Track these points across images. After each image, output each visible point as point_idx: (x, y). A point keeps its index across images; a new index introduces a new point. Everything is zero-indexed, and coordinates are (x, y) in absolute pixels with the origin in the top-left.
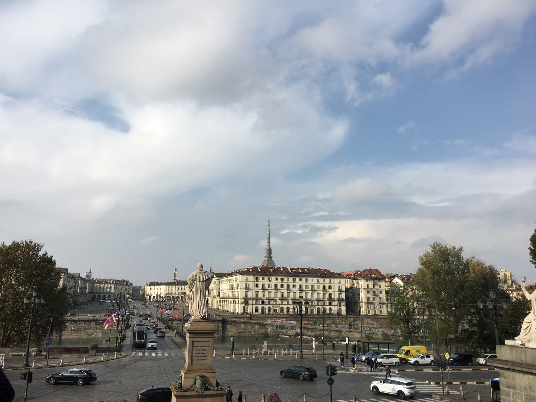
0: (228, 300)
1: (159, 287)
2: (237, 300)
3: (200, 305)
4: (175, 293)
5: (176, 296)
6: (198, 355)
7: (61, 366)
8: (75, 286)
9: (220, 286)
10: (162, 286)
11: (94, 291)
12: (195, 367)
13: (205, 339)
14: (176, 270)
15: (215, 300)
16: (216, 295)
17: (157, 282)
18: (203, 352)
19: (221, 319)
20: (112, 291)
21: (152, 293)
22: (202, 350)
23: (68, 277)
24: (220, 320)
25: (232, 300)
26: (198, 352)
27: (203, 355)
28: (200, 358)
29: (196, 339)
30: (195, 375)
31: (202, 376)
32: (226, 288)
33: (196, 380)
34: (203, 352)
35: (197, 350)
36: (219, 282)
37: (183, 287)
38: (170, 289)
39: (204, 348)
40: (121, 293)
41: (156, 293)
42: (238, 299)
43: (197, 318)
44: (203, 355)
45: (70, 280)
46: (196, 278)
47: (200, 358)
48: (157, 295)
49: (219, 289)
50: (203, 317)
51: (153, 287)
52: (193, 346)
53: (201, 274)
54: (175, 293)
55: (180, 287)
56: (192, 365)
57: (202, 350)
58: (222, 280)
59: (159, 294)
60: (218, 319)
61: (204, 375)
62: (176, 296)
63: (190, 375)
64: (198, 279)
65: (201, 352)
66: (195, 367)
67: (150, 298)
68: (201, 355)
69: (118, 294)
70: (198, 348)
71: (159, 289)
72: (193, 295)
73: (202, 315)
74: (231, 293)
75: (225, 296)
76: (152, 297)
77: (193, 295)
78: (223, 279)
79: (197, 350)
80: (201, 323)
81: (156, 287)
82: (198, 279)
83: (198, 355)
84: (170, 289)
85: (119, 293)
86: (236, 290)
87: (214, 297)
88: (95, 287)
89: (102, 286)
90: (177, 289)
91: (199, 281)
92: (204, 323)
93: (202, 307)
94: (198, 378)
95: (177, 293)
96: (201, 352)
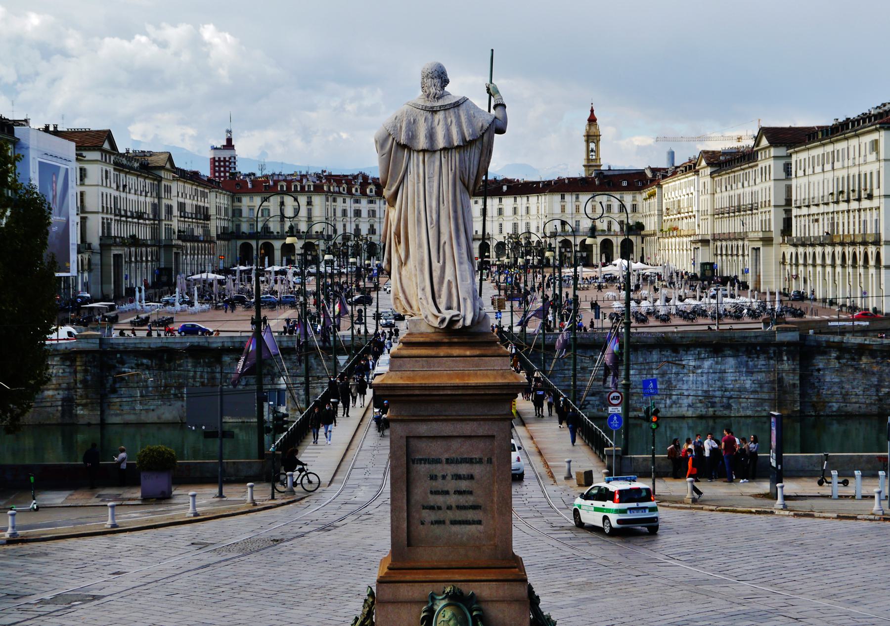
0: (829, 249)
1: (522, 201)
2: (872, 250)
3: (436, 266)
6: (440, 500)
7: (9, 542)
8: (156, 208)
9: (789, 189)
10: (533, 199)
11: (245, 228)
12: (425, 555)
13: (467, 428)
14: (592, 120)
15: (770, 255)
16: (776, 228)
17: (506, 181)
18: (464, 485)
19: (793, 336)
20: (317, 228)
21: (492, 228)
22: (458, 477)
23: (119, 167)
24: (789, 344)
25: (849, 250)
26: (439, 484)
27: (463, 500)
28: (450, 515)
29: (423, 429)
30: (428, 589)
31: (457, 599)
32: (817, 193)
33: (431, 611)
34: (464, 485)
35: (433, 477)
36: (787, 169)
37: (628, 199)
38: (569, 208)
39: (463, 469)
40: (358, 230)
41: (508, 229)
42: (877, 243)
43: (424, 328)
44: (463, 500)
45: (132, 180)
46: (412, 137)
47: (450, 515)
48: (515, 235)
49: (789, 202)
50: (452, 322)
52: (411, 460)
53: (440, 116)
56: (409, 545)
57: (458, 477)
58: (800, 157)
59: (522, 230)
60: (779, 337)
61: (469, 589)
63: (406, 592)
64: (422, 142)
65: (451, 485)
66: (425, 555)
68: (453, 499)
69: (346, 238)
70: (438, 469)
71: (522, 210)
72: (403, 220)
73: (448, 315)
74: (841, 219)
75: (818, 231)
76: (493, 244)
77: (403, 220)
78: (803, 156)
79: (433, 477)
80: (442, 351)
81: (508, 202)
82: (422, 142)
83: (440, 500)
84: (569, 208)
85: (350, 229)
86: (865, 204)
87: (767, 241)
88: (245, 213)
89: (273, 203)
91: (430, 151)
92: (456, 351)
93: (449, 276)
94: (440, 604)
95: (602, 225)
96: (451, 485)
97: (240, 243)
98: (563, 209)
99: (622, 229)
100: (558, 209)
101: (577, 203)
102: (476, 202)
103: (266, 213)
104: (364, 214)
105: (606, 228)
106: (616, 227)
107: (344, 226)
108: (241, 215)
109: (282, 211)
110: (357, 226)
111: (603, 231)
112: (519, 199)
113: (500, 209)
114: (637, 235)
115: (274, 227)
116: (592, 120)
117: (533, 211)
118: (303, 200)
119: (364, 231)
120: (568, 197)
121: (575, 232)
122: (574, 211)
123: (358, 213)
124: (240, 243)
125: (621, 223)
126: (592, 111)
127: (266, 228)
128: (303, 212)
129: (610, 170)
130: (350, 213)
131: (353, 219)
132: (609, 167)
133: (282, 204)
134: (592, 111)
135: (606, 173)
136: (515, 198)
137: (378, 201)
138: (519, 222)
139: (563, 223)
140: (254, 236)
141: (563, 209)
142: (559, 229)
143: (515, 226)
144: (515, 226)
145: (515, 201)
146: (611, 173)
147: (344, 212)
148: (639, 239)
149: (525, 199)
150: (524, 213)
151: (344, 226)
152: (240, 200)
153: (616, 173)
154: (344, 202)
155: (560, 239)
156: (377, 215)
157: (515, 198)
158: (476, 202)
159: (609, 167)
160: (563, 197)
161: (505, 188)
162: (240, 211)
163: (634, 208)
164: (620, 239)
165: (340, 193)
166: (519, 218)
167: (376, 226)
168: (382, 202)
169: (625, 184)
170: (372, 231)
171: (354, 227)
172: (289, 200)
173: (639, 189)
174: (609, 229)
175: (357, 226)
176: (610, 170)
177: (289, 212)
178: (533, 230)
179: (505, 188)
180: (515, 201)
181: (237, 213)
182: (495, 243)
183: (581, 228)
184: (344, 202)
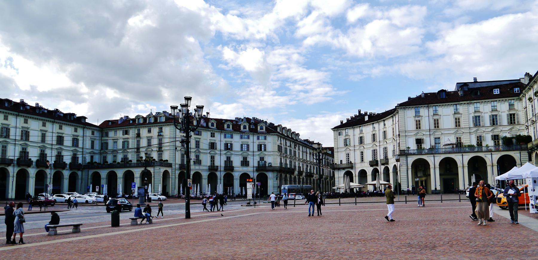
1: (379, 127)
4: (459, 147)
5: (462, 160)
11: (110, 159)
21: (355, 158)
38: (426, 124)
41: (368, 157)
51: (354, 133)
54: (459, 147)
59: (380, 157)
62: (462, 160)
76: (355, 173)
84: (426, 124)
85: (220, 161)
88: (111, 146)
90: (467, 121)
95: (469, 140)
97: (91, 172)
98: (418, 125)
99: (496, 145)
100: (411, 125)
101: (436, 117)
103: (126, 143)
104: (236, 147)
105: (474, 143)
106: (489, 142)
107: (213, 158)
108: (107, 148)
109: (138, 142)
110: (228, 158)
111: (471, 147)
113: (361, 137)
114: (521, 149)
115: (132, 157)
117: (390, 135)
118: (155, 131)
119: (236, 161)
120: (424, 111)
121: (433, 151)
122: (432, 127)
123: (228, 147)
124: (91, 172)
125: (495, 138)
127: (125, 159)
128: (155, 142)
129: (476, 82)
130: (220, 146)
131: (225, 152)
132: (475, 79)
133: (138, 135)
135: (471, 86)
137: (251, 137)
138: (378, 148)
139: (419, 142)
140: (115, 165)
141: (418, 125)
142: (413, 146)
143: (374, 152)
146: (477, 86)
147: (213, 146)
148: (525, 154)
149: (382, 124)
150: (381, 138)
151: (213, 158)
152: (107, 135)
153: (484, 85)
154: (213, 135)
155: (411, 159)
156: (251, 149)
159: (475, 79)
161: (366, 118)
162: (107, 144)
163: (512, 119)
164: (496, 156)
165: (207, 127)
166: (378, 144)
167: (250, 159)
168: (255, 137)
169: (497, 92)
170: (245, 163)
171: (224, 158)
172: (144, 132)
173: (518, 96)
174: (480, 144)
175: (228, 158)
176: (476, 82)
177: (144, 143)
178: (390, 155)
179: (366, 118)
181: (104, 146)
182: (358, 171)
183: (441, 146)
184: (213, 135)
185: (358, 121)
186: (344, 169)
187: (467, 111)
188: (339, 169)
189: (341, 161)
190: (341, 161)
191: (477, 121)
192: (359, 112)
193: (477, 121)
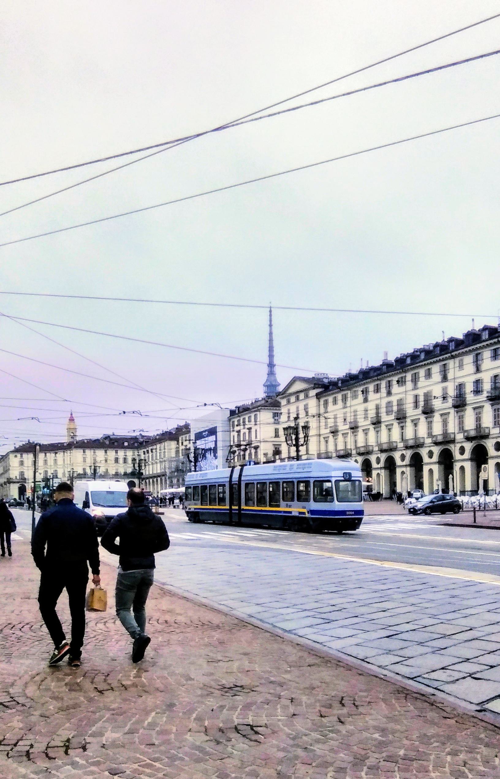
14: (72, 420)
21: (29, 475)
55: (121, 453)
67: (22, 490)
102: (16, 456)
112: (48, 454)
116: (72, 420)
120: (89, 453)
126: (71, 414)
129: (114, 435)
132: (113, 433)
134: (71, 414)
136: (46, 453)
144: (46, 472)
145: (46, 455)
153: (118, 437)
157: (46, 453)
158: (16, 456)
160: (84, 452)
180: (46, 455)
185: (30, 448)
186: (18, 482)
187: (111, 454)
188: (14, 482)
189: (16, 477)
190: (16, 477)
191: (117, 460)
192: (29, 441)
193: (117, 460)
